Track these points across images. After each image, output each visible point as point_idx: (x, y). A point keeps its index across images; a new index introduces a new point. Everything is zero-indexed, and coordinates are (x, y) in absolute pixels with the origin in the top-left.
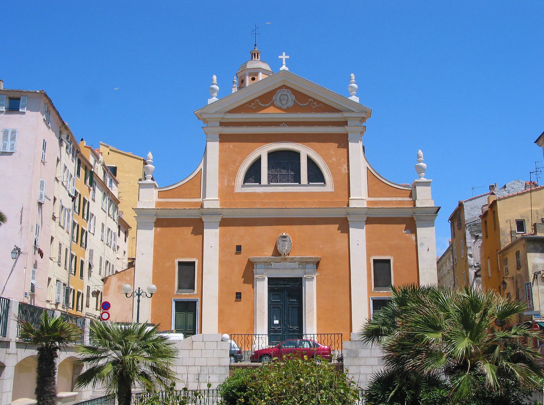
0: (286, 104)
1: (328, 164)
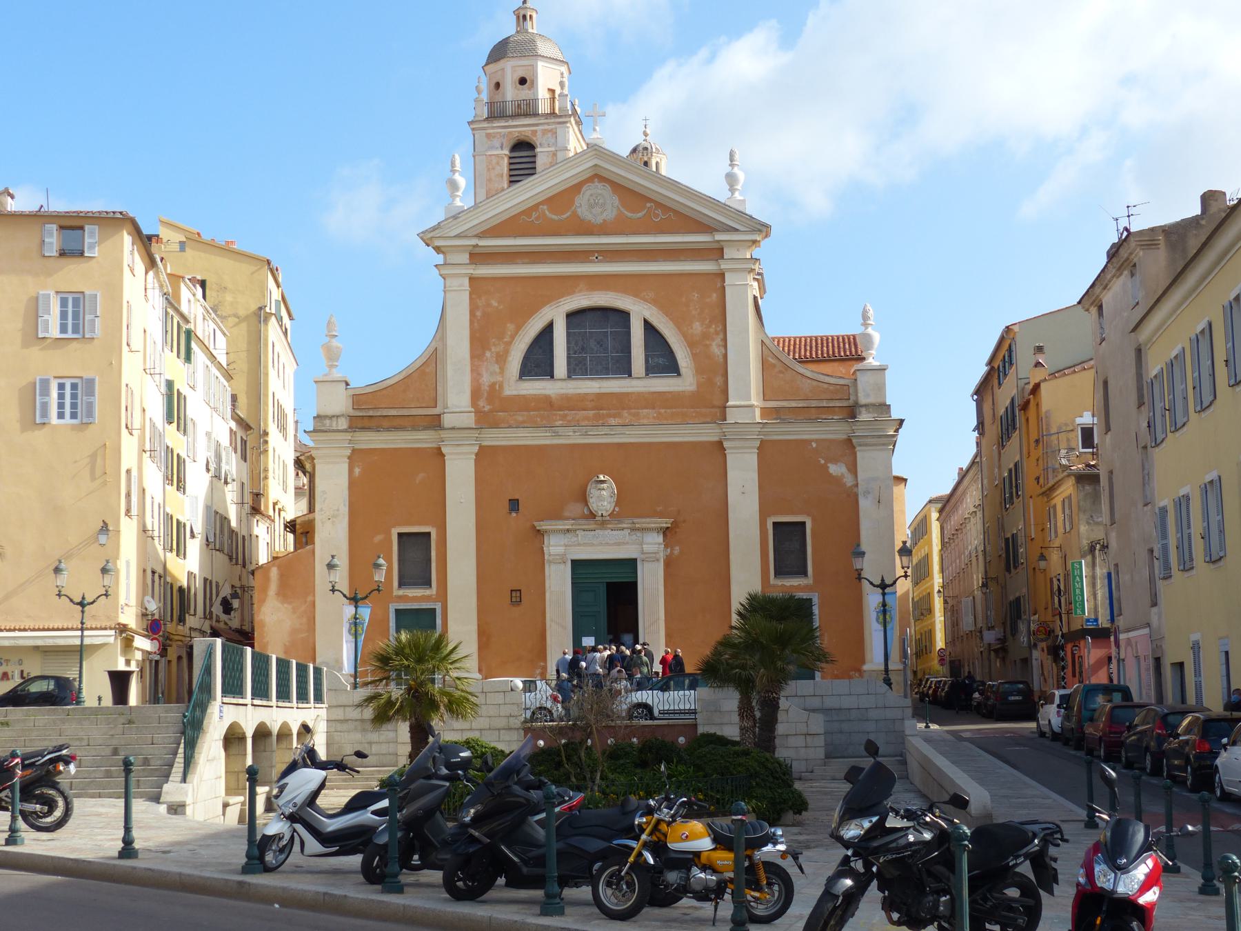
1: (685, 336)
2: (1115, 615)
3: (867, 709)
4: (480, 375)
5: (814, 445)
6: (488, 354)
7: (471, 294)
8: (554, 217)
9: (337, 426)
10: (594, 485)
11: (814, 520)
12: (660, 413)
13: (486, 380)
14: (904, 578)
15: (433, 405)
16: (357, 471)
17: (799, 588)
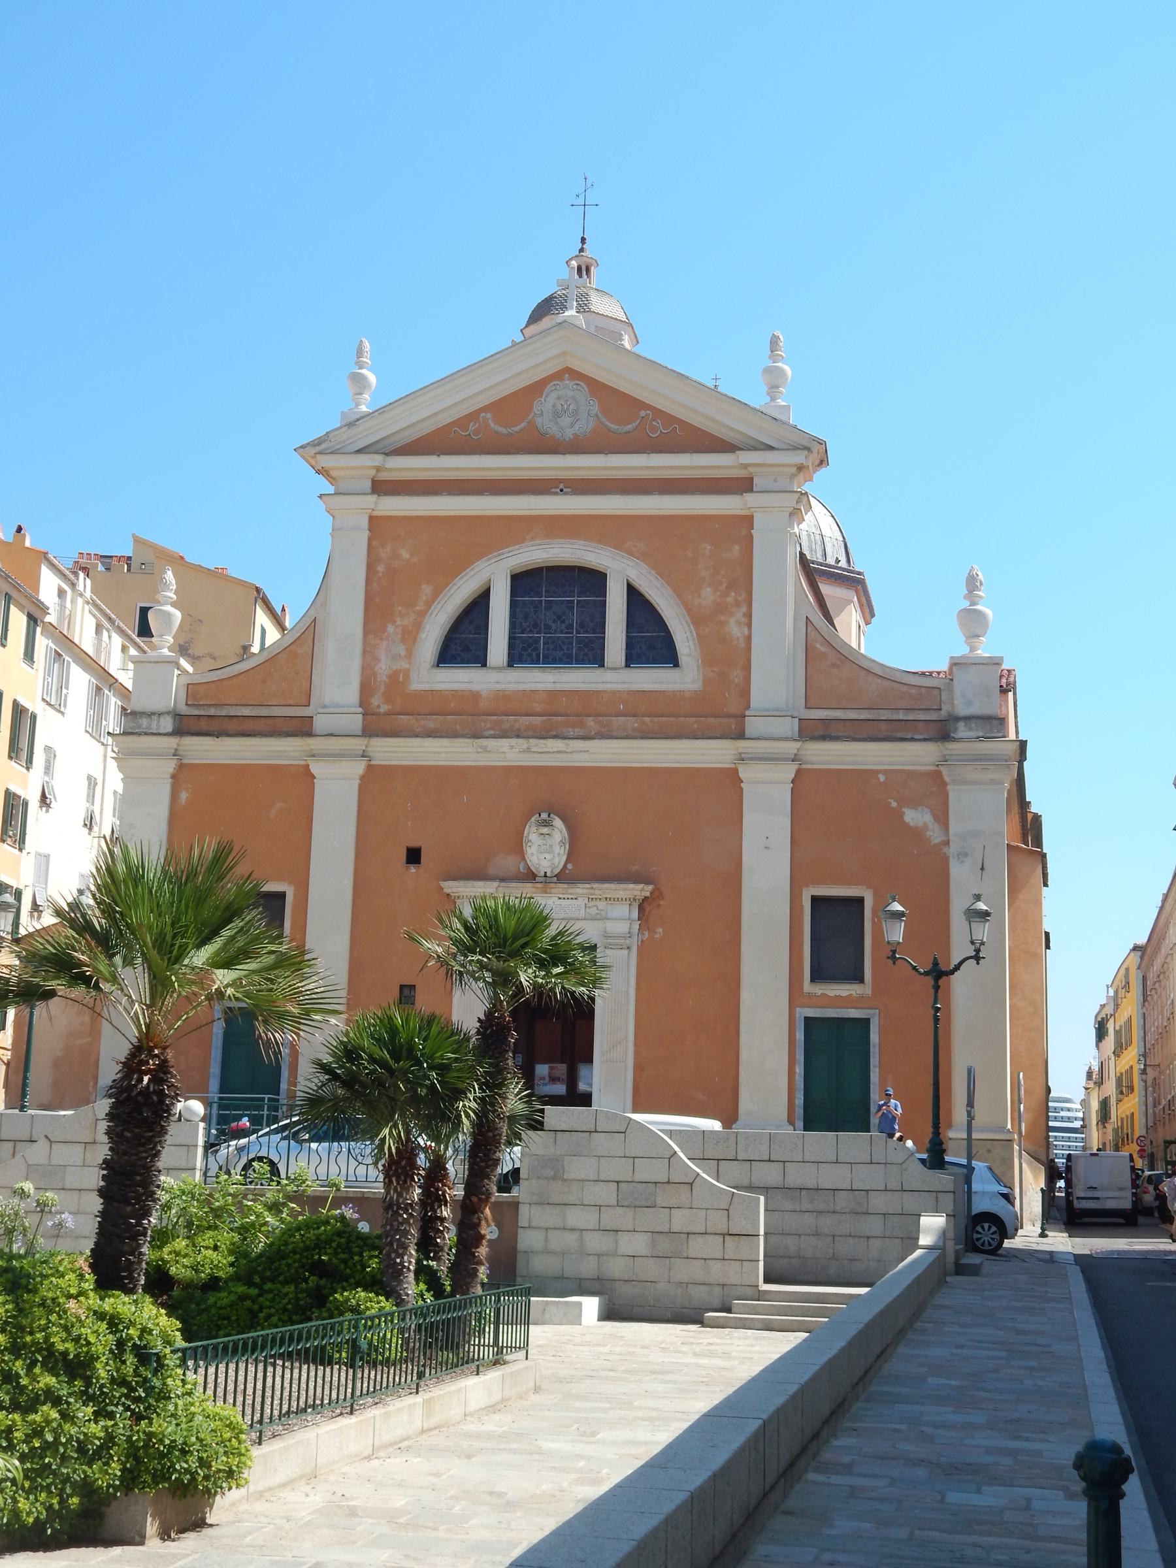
0: (572, 425)
1: (688, 610)
3: (867, 1191)
4: (376, 659)
5: (882, 778)
6: (390, 629)
7: (370, 540)
11: (875, 896)
13: (384, 667)
15: (304, 702)
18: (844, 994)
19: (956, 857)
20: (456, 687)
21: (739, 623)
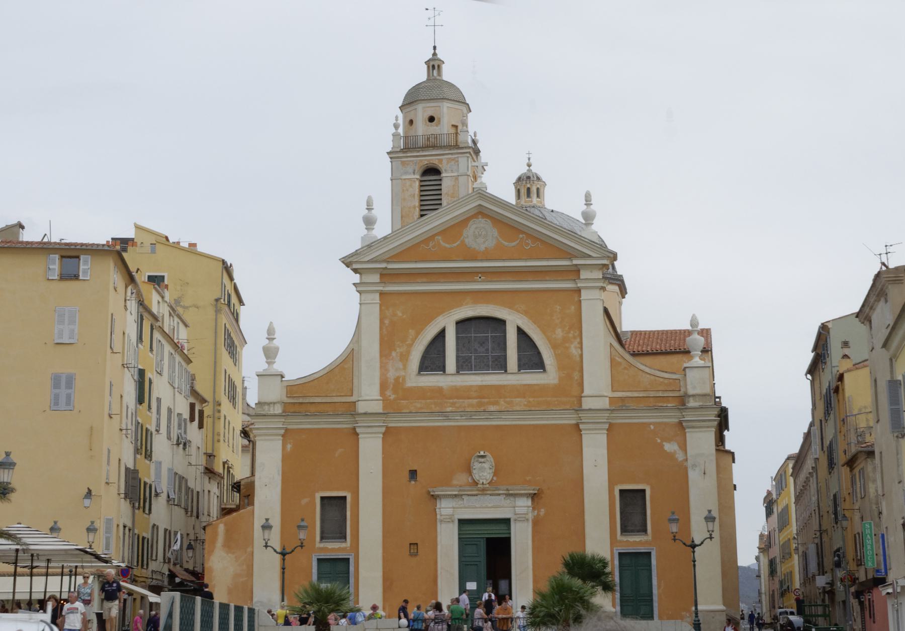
0: (484, 242)
1: (549, 339)
2: (888, 568)
5: (652, 427)
6: (394, 354)
7: (381, 306)
8: (447, 246)
9: (274, 409)
10: (476, 459)
11: (652, 489)
12: (529, 402)
13: (392, 375)
14: (709, 540)
16: (289, 447)
17: (640, 543)
18: (638, 540)
19: (691, 468)
20: (430, 384)
21: (576, 348)
